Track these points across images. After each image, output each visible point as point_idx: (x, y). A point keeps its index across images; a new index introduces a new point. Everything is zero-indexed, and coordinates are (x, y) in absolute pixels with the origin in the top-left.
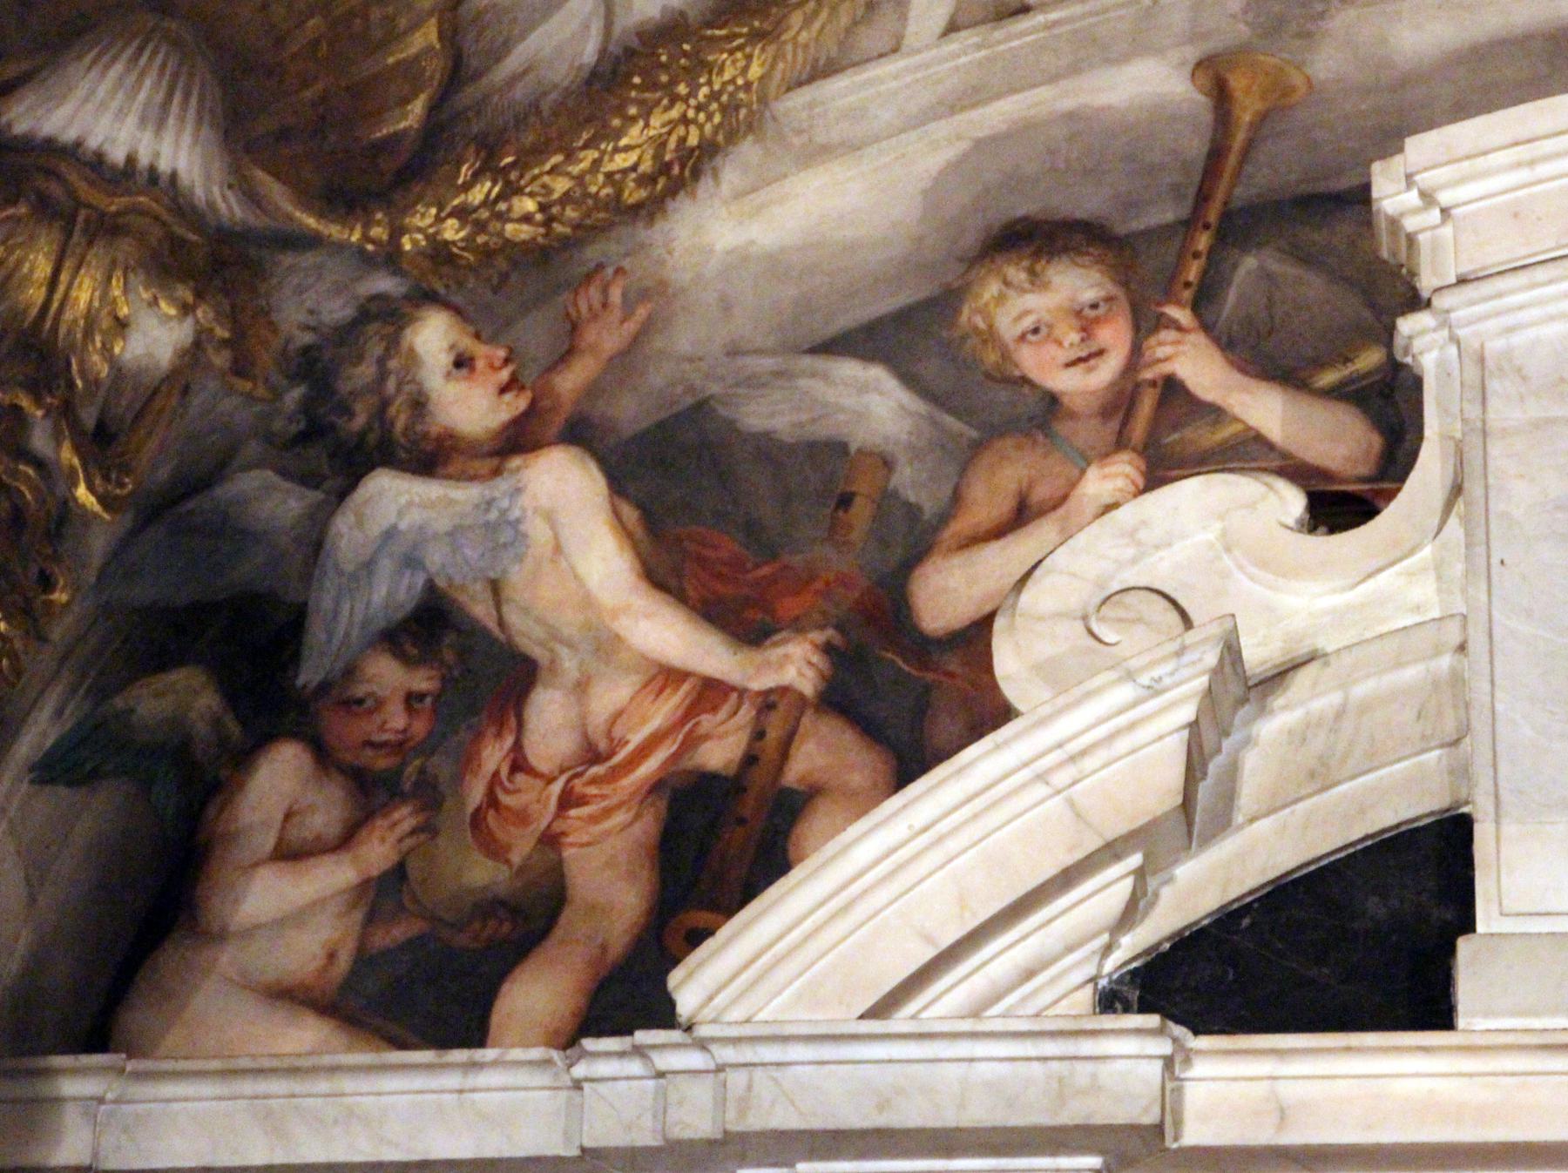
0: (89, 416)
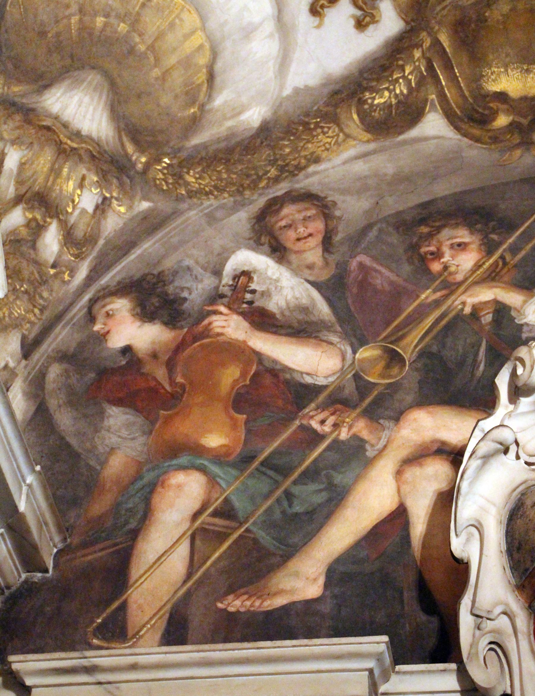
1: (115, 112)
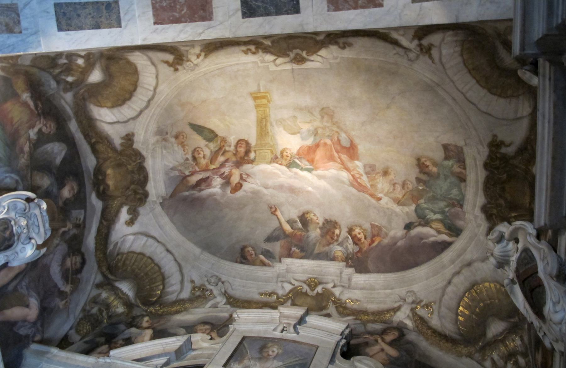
0: (110, 314)
1: (502, 319)
